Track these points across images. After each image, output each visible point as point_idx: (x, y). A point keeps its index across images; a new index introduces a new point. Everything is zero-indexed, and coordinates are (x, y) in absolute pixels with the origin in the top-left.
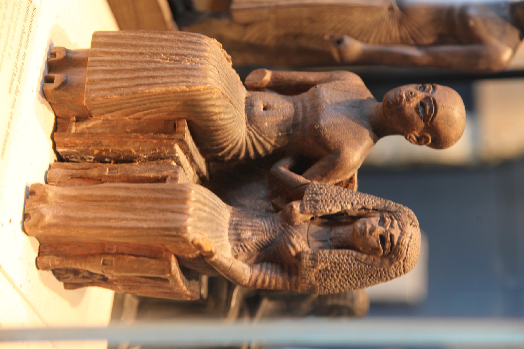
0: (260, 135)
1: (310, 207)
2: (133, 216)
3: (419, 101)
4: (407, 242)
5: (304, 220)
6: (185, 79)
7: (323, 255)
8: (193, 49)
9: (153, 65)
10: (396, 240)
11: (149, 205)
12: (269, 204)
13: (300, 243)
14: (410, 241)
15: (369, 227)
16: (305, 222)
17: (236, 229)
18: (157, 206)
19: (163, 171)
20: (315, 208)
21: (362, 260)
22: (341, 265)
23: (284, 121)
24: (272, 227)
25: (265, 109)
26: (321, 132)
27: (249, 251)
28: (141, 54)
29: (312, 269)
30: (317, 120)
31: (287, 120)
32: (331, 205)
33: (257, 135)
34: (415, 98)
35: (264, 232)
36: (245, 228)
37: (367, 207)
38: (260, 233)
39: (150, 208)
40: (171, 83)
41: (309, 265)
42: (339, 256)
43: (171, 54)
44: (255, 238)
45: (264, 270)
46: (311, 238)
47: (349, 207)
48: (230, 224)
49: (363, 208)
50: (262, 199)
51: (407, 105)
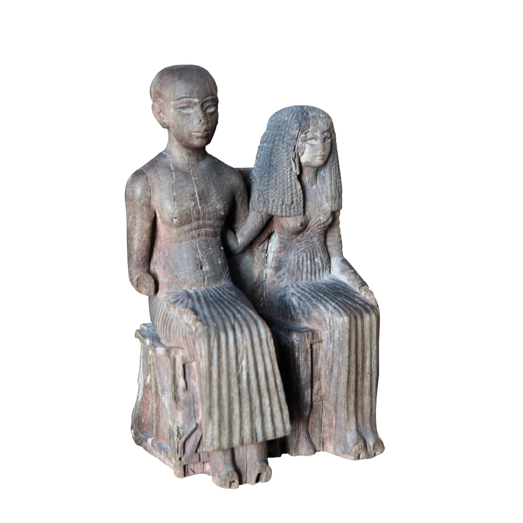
12: (257, 250)
19: (307, 348)
50: (253, 258)
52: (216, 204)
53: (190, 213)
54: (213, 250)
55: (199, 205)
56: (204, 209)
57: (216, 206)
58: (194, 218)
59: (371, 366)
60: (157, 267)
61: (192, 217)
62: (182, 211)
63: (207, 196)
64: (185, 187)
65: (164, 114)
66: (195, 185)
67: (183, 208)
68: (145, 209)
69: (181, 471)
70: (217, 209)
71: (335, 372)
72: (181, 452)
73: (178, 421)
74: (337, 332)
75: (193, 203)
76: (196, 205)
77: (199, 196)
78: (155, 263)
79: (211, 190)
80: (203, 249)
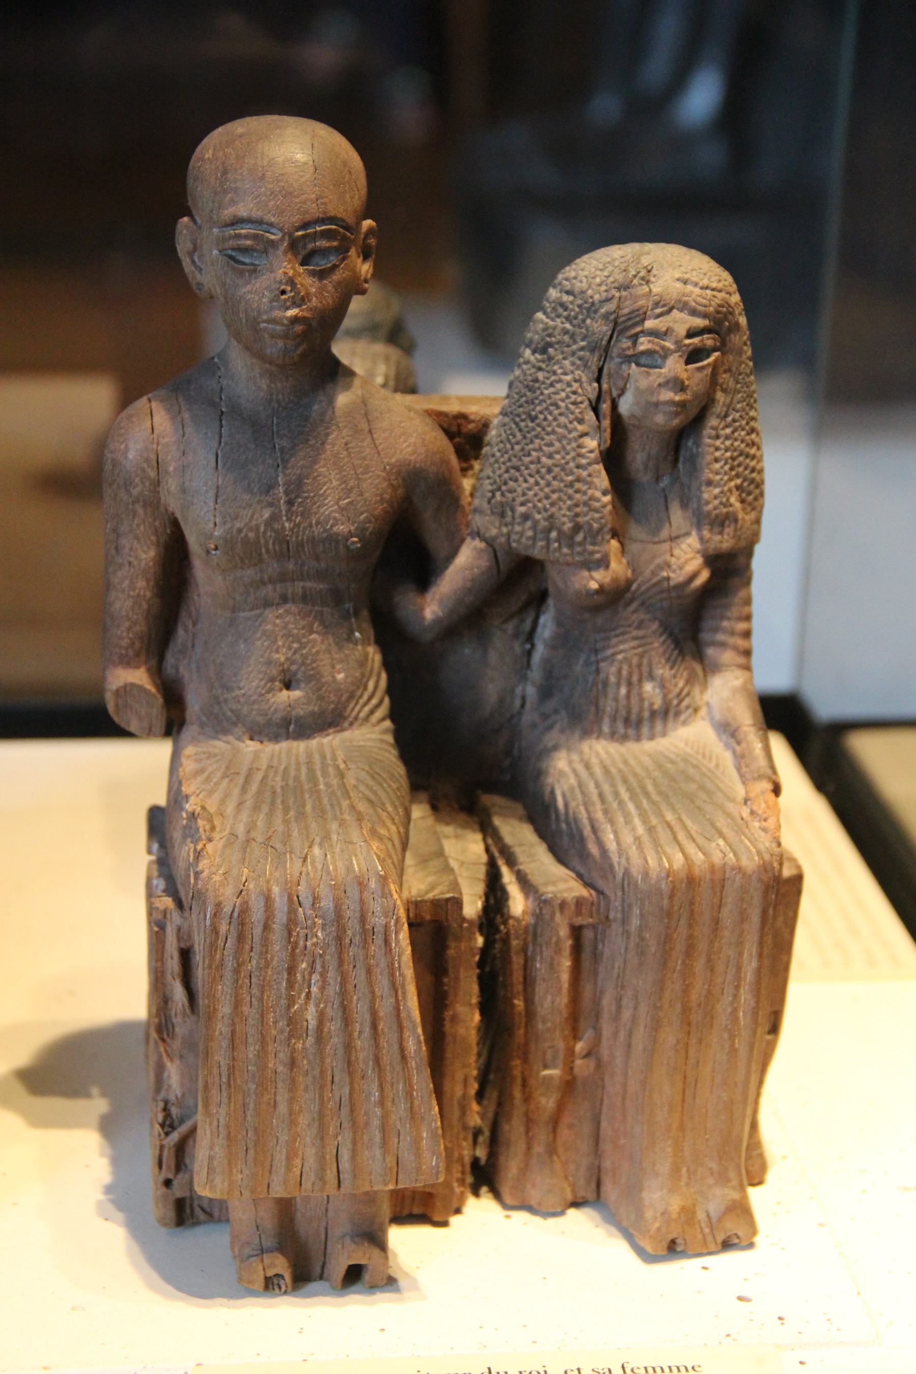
0: (365, 688)
1: (594, 544)
2: (728, 998)
3: (301, 269)
4: (697, 291)
5: (620, 555)
6: (379, 939)
7: (716, 502)
8: (266, 927)
9: (334, 1027)
10: (700, 322)
11: (699, 965)
13: (682, 560)
14: (696, 285)
15: (667, 395)
16: (623, 552)
17: (639, 722)
18: (702, 946)
20: (600, 530)
21: (728, 400)
22: (735, 454)
23: (327, 628)
24: (629, 632)
25: (288, 686)
26: (370, 530)
27: (687, 682)
28: (292, 1063)
29: (740, 523)
30: (333, 540)
31: (322, 622)
32: (590, 492)
33: (365, 697)
34: (298, 280)
35: (645, 652)
36: (634, 701)
37: (593, 397)
38: (645, 661)
39: (709, 960)
40: (392, 975)
41: (732, 534)
42: (716, 460)
43: (291, 985)
44: (661, 671)
45: (720, 637)
46: (665, 533)
47: (592, 443)
48: (625, 738)
49: (596, 410)
50: (485, 652)
51: (314, 302)
52: (335, 518)
53: (258, 537)
54: (322, 642)
55: (284, 518)
56: (298, 532)
57: (332, 526)
58: (267, 551)
59: (735, 1010)
60: (185, 662)
61: (263, 550)
62: (235, 531)
63: (312, 494)
64: (250, 466)
65: (201, 257)
66: (279, 460)
67: (238, 525)
68: (141, 511)
69: (171, 1214)
70: (337, 534)
71: (627, 1014)
72: (169, 1167)
73: (170, 1086)
74: (636, 911)
75: (267, 514)
76: (274, 518)
77: (286, 493)
78: (180, 652)
79: (326, 480)
80: (293, 636)
